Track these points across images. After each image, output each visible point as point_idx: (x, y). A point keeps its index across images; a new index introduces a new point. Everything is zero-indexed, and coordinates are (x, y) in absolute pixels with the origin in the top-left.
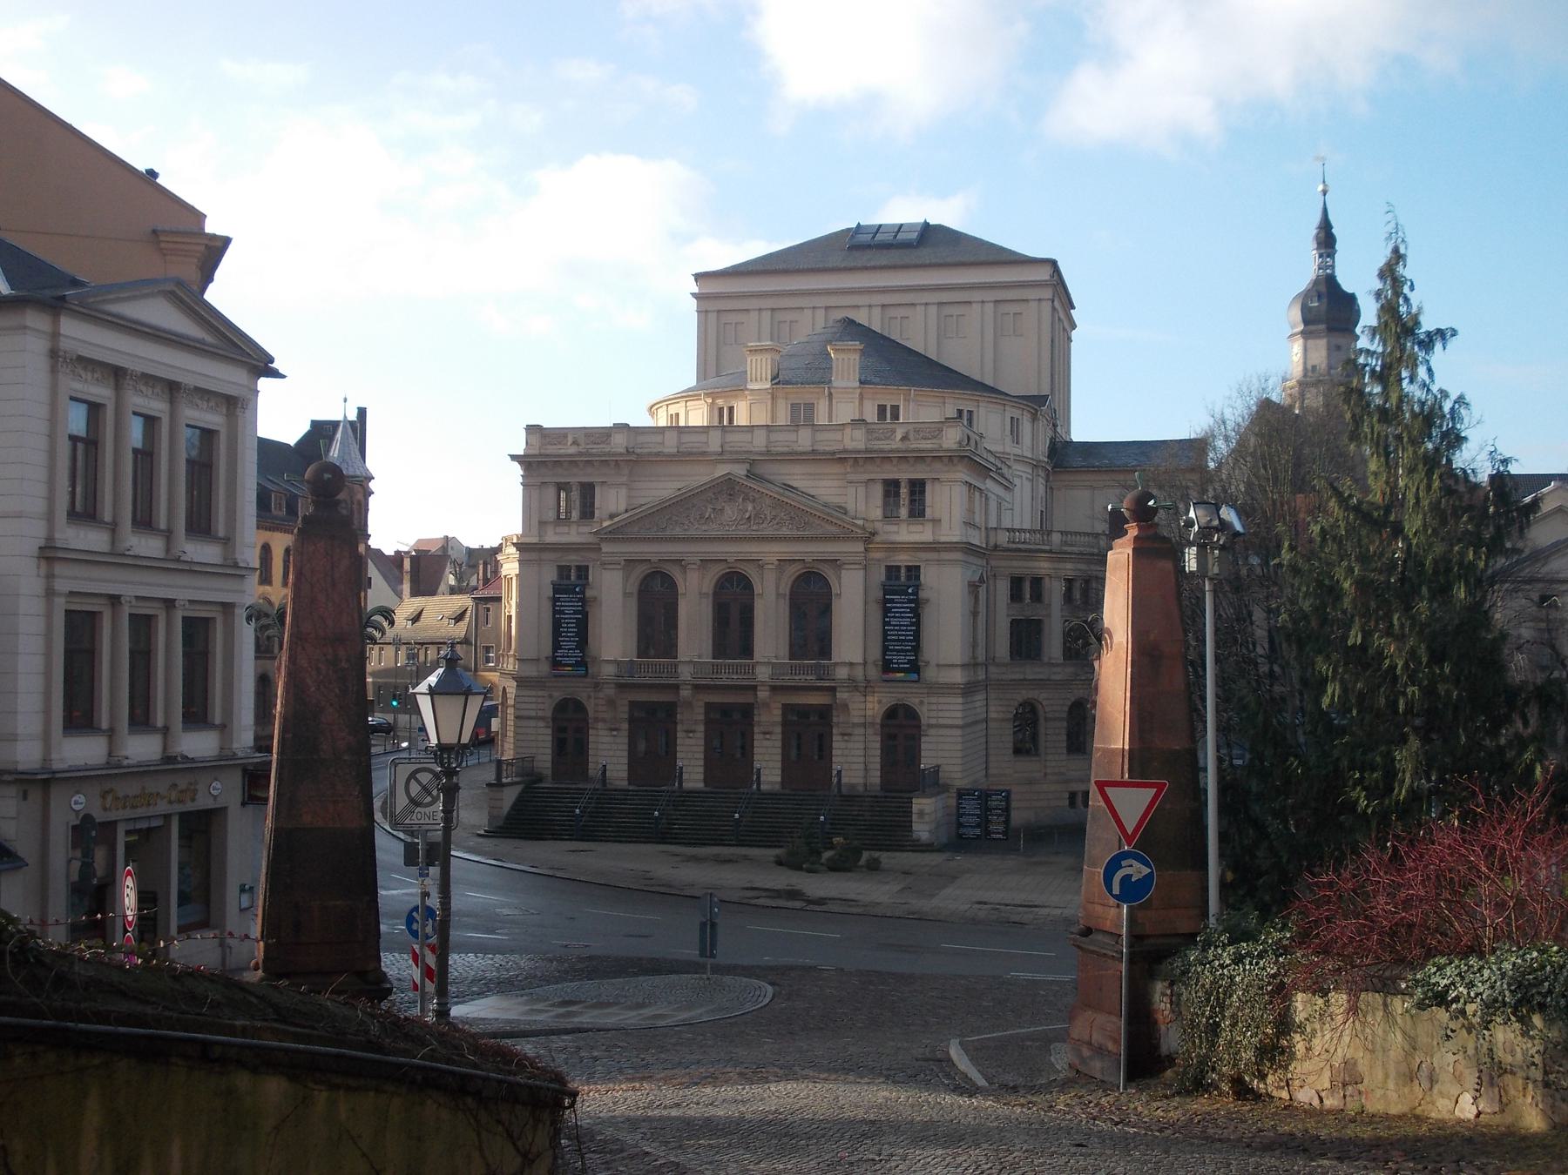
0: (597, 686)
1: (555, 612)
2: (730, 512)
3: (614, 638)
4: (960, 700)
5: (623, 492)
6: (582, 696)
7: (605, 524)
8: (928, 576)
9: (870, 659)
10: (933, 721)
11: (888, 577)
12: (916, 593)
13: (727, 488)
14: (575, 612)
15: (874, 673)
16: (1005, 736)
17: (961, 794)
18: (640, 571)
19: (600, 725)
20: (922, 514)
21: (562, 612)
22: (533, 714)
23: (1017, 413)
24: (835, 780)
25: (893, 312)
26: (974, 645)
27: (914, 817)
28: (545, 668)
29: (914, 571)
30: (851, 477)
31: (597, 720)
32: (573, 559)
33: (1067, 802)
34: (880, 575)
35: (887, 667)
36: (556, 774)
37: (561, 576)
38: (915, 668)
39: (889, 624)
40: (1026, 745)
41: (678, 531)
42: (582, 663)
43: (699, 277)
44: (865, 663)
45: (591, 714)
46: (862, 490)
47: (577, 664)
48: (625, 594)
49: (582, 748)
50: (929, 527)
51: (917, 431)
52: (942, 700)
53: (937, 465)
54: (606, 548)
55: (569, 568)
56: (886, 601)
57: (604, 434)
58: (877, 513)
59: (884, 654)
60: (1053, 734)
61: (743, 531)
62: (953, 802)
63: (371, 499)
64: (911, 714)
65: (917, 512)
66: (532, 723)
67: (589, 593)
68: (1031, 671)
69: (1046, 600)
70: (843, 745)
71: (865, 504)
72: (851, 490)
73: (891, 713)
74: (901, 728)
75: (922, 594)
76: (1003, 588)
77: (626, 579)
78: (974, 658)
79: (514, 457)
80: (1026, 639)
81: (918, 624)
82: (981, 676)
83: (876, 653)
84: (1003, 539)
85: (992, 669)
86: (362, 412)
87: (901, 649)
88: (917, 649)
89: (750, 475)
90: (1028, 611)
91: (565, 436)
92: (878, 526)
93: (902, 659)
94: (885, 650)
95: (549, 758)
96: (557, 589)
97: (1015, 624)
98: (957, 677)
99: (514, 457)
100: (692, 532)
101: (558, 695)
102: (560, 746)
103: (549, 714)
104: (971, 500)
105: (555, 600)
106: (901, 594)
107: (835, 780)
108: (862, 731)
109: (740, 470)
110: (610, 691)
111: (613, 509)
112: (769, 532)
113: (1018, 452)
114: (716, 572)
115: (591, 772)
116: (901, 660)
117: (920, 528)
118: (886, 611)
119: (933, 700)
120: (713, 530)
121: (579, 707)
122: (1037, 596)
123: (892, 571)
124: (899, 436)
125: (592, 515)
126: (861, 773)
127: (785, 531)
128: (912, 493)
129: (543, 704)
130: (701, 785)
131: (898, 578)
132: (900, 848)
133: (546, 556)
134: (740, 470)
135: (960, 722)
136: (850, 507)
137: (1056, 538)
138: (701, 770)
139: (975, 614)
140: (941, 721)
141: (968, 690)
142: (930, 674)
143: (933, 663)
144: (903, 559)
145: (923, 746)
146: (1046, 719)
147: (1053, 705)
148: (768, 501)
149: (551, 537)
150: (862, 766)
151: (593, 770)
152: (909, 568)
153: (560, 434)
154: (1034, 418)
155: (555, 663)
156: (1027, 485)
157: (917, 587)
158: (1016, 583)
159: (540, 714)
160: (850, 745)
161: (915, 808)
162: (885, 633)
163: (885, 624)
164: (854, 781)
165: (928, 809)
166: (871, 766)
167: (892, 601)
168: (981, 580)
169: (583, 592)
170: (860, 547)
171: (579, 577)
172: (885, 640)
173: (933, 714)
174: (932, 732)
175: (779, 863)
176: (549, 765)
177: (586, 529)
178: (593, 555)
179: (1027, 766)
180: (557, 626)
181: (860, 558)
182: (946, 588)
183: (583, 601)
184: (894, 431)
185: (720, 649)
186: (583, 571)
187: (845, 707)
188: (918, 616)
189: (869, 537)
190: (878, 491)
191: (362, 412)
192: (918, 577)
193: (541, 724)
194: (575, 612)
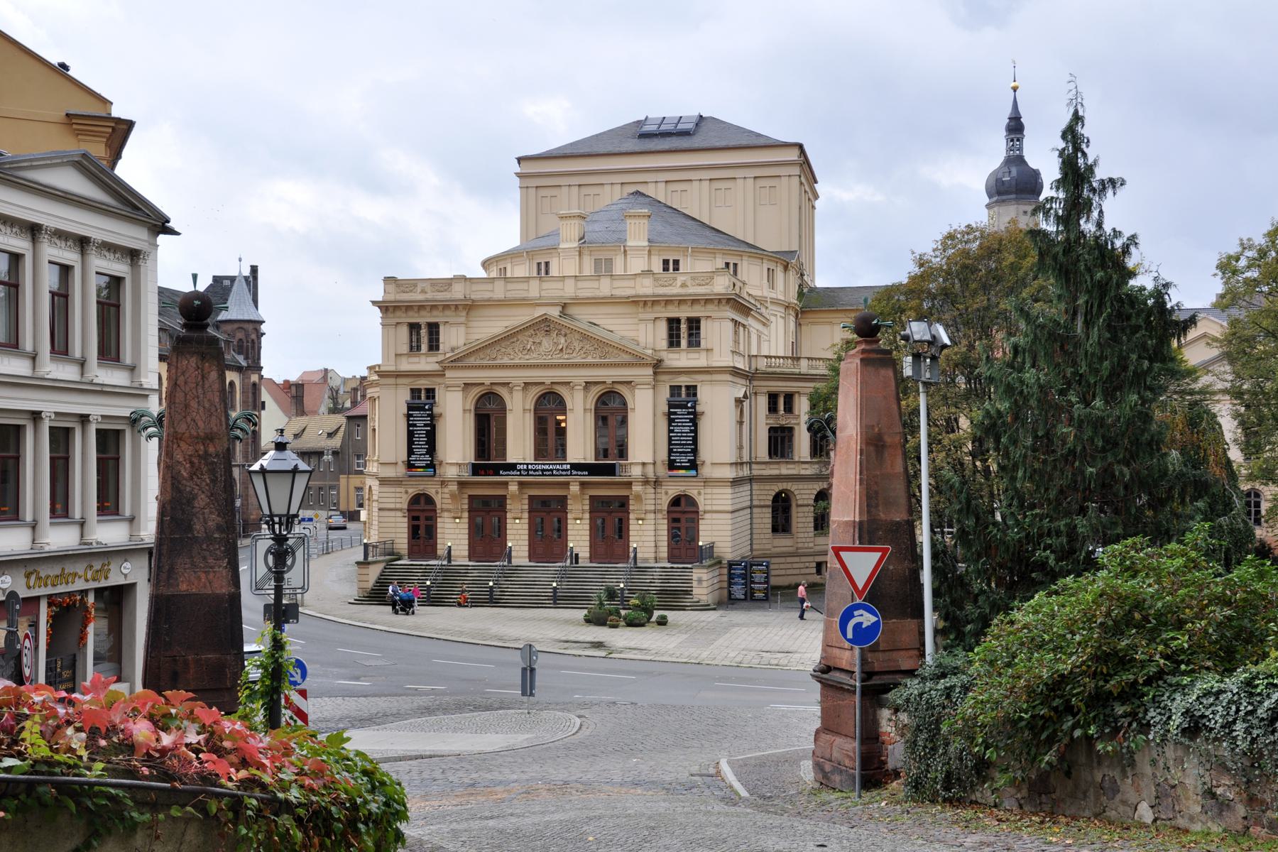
0: (443, 483)
1: (409, 425)
2: (547, 344)
3: (457, 445)
4: (729, 490)
5: (462, 329)
6: (431, 492)
8: (704, 394)
9: (659, 463)
10: (708, 508)
11: (672, 395)
12: (694, 407)
13: (544, 325)
14: (426, 425)
15: (663, 471)
16: (765, 518)
17: (731, 565)
18: (475, 393)
19: (446, 514)
20: (698, 344)
21: (415, 425)
22: (392, 506)
23: (772, 266)
24: (632, 555)
25: (672, 187)
26: (741, 448)
27: (695, 584)
28: (401, 470)
29: (692, 390)
31: (442, 510)
32: (423, 384)
33: (814, 570)
34: (665, 393)
35: (672, 465)
36: (412, 554)
37: (413, 398)
38: (693, 465)
39: (671, 431)
40: (781, 524)
41: (506, 361)
42: (431, 465)
43: (520, 160)
44: (654, 464)
45: (439, 506)
46: (650, 326)
47: (427, 466)
48: (464, 411)
49: (431, 532)
50: (704, 354)
51: (693, 279)
52: (715, 491)
53: (710, 307)
54: (448, 374)
55: (420, 390)
56: (670, 413)
57: (448, 283)
58: (663, 344)
59: (670, 456)
60: (802, 519)
62: (725, 571)
63: (263, 339)
64: (692, 502)
65: (694, 342)
66: (392, 513)
67: (436, 410)
68: (785, 470)
70: (638, 527)
71: (651, 336)
72: (642, 326)
73: (676, 502)
74: (682, 514)
75: (699, 409)
76: (763, 402)
77: (465, 398)
78: (741, 457)
79: (374, 303)
80: (780, 441)
81: (695, 431)
82: (745, 472)
83: (663, 455)
84: (762, 364)
85: (754, 466)
86: (254, 270)
87: (684, 453)
88: (695, 451)
89: (563, 314)
90: (783, 420)
91: (415, 286)
92: (664, 355)
93: (684, 459)
94: (670, 451)
95: (406, 541)
96: (410, 408)
97: (771, 429)
98: (730, 473)
99: (374, 303)
100: (517, 361)
101: (413, 491)
102: (414, 532)
103: (406, 506)
104: (736, 333)
105: (409, 416)
106: (683, 409)
107: (632, 555)
108: (652, 516)
109: (554, 312)
110: (454, 488)
111: (454, 344)
113: (774, 296)
114: (534, 392)
115: (439, 552)
116: (684, 459)
117: (696, 355)
118: (671, 421)
119: (709, 490)
120: (533, 359)
121: (429, 500)
122: (789, 408)
123: (675, 390)
124: (679, 284)
125: (438, 349)
126: (653, 550)
127: (590, 360)
128: (690, 328)
129: (400, 498)
130: (525, 562)
131: (680, 395)
132: (683, 608)
133: (400, 381)
134: (554, 312)
135: (730, 508)
136: (642, 340)
137: (804, 363)
138: (527, 548)
139: (741, 423)
140: (715, 508)
141: (736, 482)
142: (706, 471)
143: (708, 462)
144: (683, 381)
145: (701, 527)
146: (798, 506)
147: (804, 494)
148: (577, 336)
149: (406, 365)
150: (653, 544)
151: (441, 551)
152: (688, 387)
153: (412, 284)
154: (786, 268)
155: (410, 466)
156: (781, 321)
157: (695, 402)
158: (773, 398)
159: (398, 506)
160: (644, 527)
161: (695, 577)
162: (670, 439)
163: (670, 431)
164: (646, 556)
165: (705, 577)
167: (675, 413)
168: (745, 396)
169: (431, 409)
170: (650, 371)
171: (428, 398)
172: (670, 444)
173: (709, 502)
174: (707, 516)
175: (588, 621)
176: (406, 546)
177: (435, 359)
178: (439, 380)
179: (783, 543)
180: (411, 435)
181: (650, 379)
182: (718, 404)
183: (432, 416)
184: (675, 279)
185: (540, 453)
186: (431, 393)
187: (639, 498)
188: (695, 425)
189: (657, 366)
190: (663, 328)
191: (254, 270)
192: (695, 395)
193: (399, 514)
194: (426, 425)
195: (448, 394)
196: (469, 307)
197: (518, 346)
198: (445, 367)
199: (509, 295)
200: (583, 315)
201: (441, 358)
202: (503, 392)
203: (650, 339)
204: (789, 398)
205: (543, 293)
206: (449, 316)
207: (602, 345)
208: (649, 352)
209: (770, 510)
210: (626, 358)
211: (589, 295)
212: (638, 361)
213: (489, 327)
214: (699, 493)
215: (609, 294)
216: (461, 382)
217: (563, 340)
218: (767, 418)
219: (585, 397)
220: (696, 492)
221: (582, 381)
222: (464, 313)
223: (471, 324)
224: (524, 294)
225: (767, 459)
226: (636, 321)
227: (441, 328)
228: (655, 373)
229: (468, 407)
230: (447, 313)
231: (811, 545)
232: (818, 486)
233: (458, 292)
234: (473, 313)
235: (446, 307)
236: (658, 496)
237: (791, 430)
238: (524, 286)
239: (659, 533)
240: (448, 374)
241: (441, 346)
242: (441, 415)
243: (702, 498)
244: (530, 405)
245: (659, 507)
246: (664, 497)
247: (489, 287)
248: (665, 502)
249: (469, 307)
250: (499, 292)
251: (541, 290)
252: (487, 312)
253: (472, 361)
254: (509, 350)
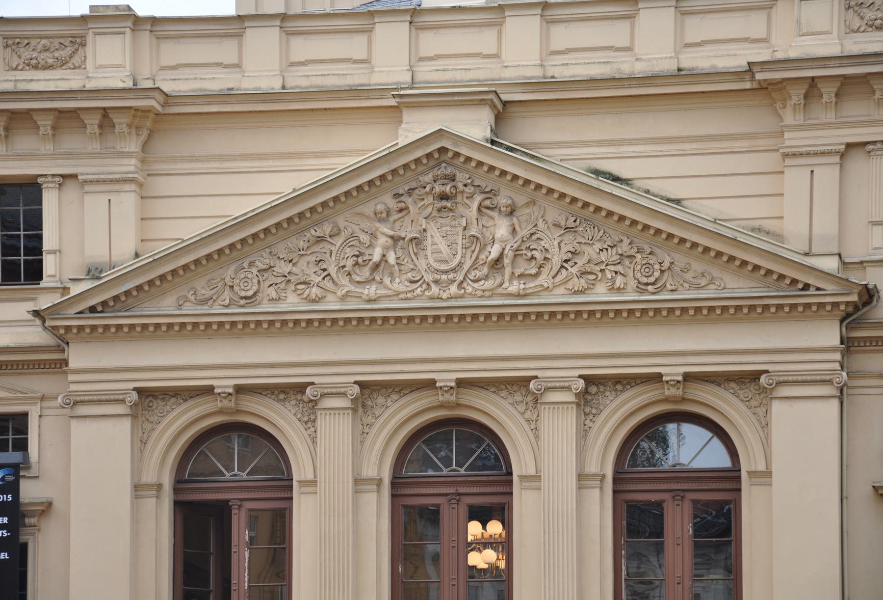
2: (441, 242)
5: (127, 202)
7: (76, 289)
18: (178, 424)
30: (793, 140)
41: (292, 302)
46: (827, 175)
48: (138, 488)
54: (79, 357)
61: (479, 294)
67: (29, 491)
72: (796, 178)
109: (474, 126)
111: (97, 252)
112: (559, 296)
120: (392, 292)
125: (35, 273)
127: (601, 294)
134: (474, 126)
148: (555, 213)
170: (829, 335)
177: (20, 310)
195: (82, 433)
196: (151, 120)
197: (337, 254)
198: (64, 331)
199: (299, 80)
200: (569, 147)
201: (44, 302)
202: (281, 420)
203: (826, 223)
205: (426, 72)
206: (79, 154)
207: (655, 234)
208: (830, 264)
210: (738, 286)
211: (595, 71)
212: (785, 293)
213: (222, 190)
215: (669, 66)
216: (127, 386)
217: (501, 229)
219: (583, 433)
221: (572, 374)
222: (133, 145)
223: (163, 186)
224: (356, 77)
226: (771, 161)
227: (50, 201)
228: (848, 345)
229: (149, 477)
230: (71, 142)
233: (109, 65)
234: (165, 146)
235: (67, 119)
238: (354, 47)
240: (79, 357)
241: (49, 264)
242: (47, 507)
244: (379, 464)
247: (226, 51)
249: (151, 120)
250: (261, 66)
251: (416, 59)
252: (217, 142)
253: (166, 306)
254: (305, 268)
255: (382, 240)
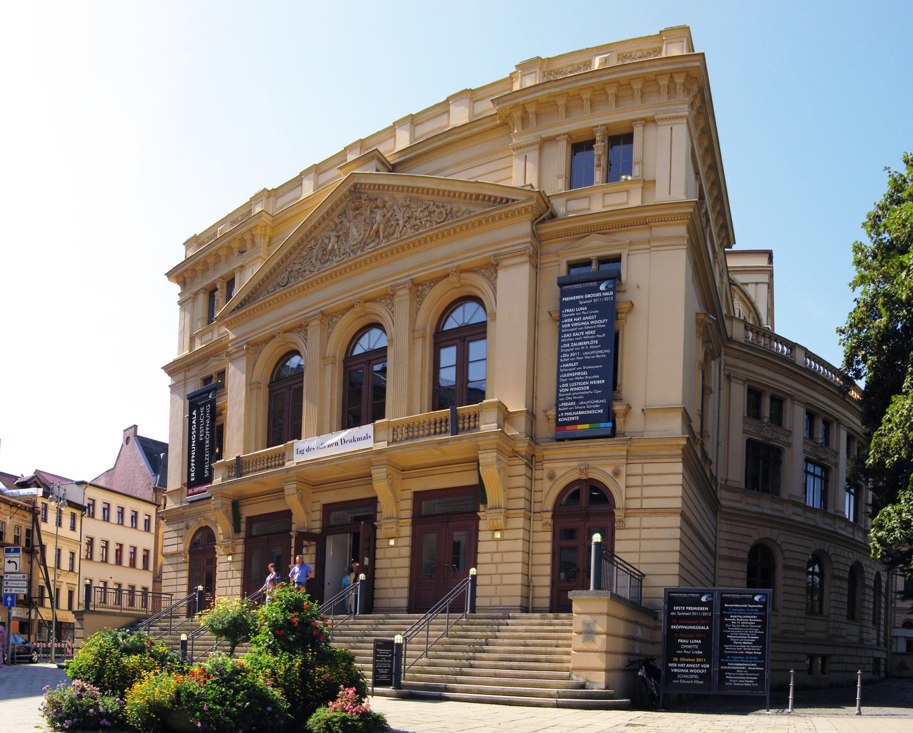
10: (635, 504)
52: (649, 468)
69: (787, 425)
70: (492, 546)
90: (767, 434)
97: (749, 442)
119: (637, 469)
122: (777, 418)
140: (647, 504)
143: (637, 410)
160: (504, 546)
166: (536, 581)
173: (635, 492)
204: (778, 402)
209: (745, 567)
214: (616, 473)
218: (745, 423)
220: (609, 470)
225: (743, 486)
231: (802, 628)
232: (816, 545)
236: (537, 485)
237: (778, 452)
239: (537, 559)
243: (622, 481)
245: (537, 507)
246: (547, 484)
248: (549, 494)
255: (333, 239)
